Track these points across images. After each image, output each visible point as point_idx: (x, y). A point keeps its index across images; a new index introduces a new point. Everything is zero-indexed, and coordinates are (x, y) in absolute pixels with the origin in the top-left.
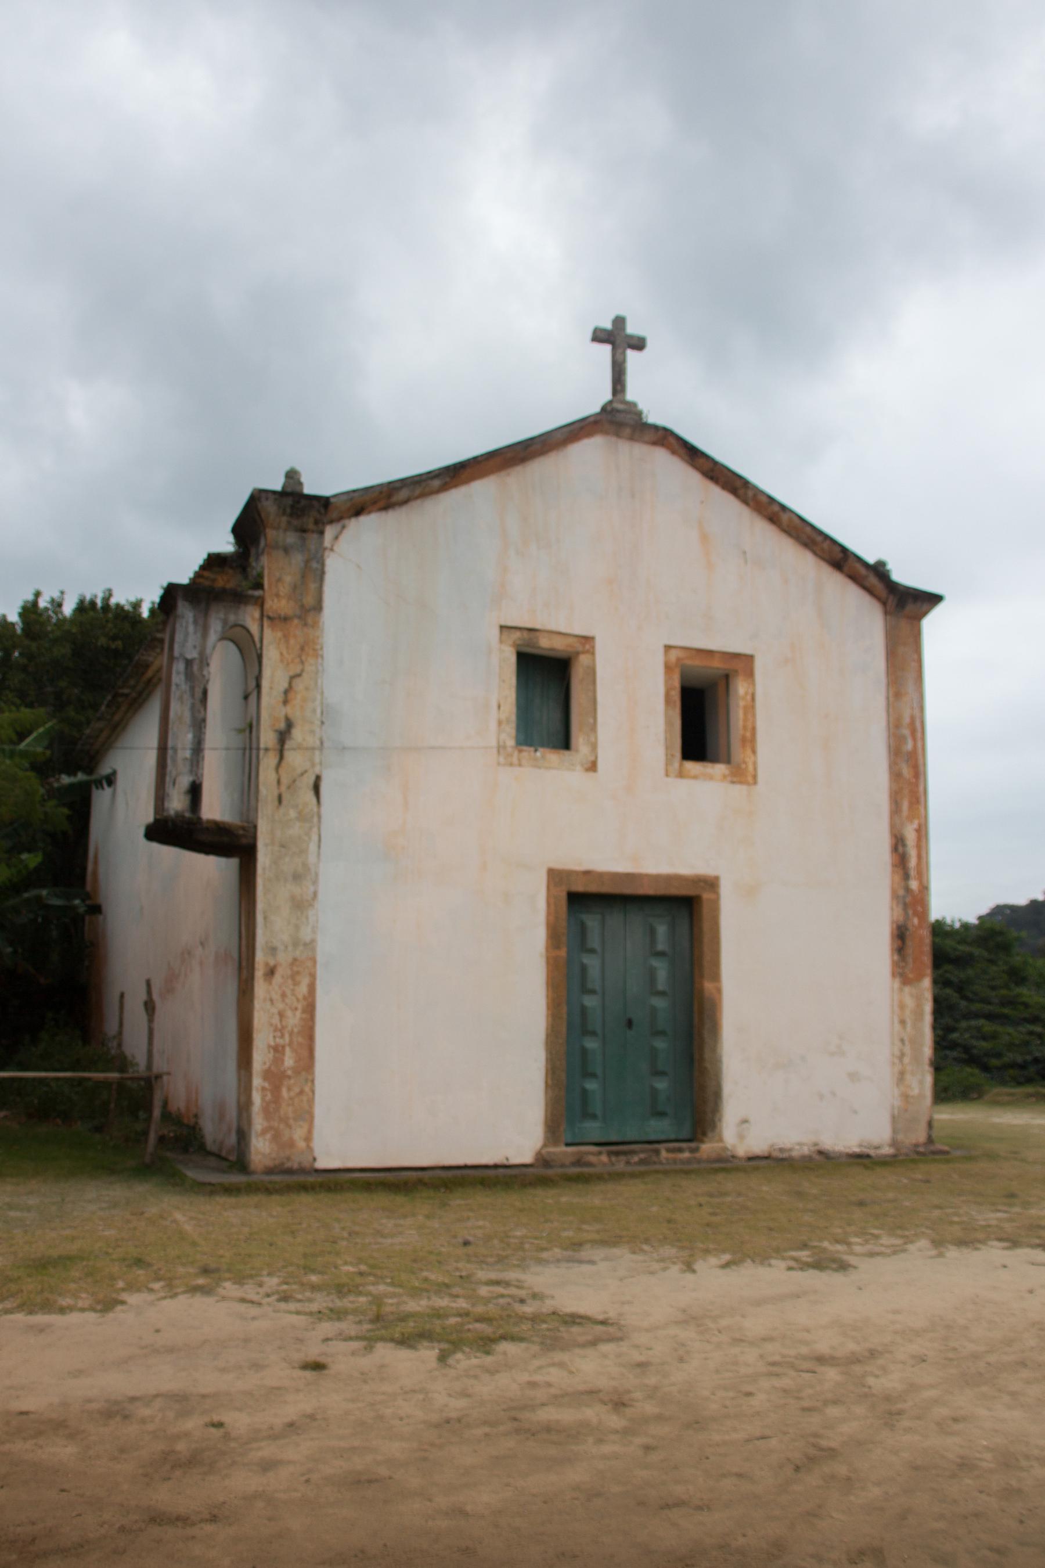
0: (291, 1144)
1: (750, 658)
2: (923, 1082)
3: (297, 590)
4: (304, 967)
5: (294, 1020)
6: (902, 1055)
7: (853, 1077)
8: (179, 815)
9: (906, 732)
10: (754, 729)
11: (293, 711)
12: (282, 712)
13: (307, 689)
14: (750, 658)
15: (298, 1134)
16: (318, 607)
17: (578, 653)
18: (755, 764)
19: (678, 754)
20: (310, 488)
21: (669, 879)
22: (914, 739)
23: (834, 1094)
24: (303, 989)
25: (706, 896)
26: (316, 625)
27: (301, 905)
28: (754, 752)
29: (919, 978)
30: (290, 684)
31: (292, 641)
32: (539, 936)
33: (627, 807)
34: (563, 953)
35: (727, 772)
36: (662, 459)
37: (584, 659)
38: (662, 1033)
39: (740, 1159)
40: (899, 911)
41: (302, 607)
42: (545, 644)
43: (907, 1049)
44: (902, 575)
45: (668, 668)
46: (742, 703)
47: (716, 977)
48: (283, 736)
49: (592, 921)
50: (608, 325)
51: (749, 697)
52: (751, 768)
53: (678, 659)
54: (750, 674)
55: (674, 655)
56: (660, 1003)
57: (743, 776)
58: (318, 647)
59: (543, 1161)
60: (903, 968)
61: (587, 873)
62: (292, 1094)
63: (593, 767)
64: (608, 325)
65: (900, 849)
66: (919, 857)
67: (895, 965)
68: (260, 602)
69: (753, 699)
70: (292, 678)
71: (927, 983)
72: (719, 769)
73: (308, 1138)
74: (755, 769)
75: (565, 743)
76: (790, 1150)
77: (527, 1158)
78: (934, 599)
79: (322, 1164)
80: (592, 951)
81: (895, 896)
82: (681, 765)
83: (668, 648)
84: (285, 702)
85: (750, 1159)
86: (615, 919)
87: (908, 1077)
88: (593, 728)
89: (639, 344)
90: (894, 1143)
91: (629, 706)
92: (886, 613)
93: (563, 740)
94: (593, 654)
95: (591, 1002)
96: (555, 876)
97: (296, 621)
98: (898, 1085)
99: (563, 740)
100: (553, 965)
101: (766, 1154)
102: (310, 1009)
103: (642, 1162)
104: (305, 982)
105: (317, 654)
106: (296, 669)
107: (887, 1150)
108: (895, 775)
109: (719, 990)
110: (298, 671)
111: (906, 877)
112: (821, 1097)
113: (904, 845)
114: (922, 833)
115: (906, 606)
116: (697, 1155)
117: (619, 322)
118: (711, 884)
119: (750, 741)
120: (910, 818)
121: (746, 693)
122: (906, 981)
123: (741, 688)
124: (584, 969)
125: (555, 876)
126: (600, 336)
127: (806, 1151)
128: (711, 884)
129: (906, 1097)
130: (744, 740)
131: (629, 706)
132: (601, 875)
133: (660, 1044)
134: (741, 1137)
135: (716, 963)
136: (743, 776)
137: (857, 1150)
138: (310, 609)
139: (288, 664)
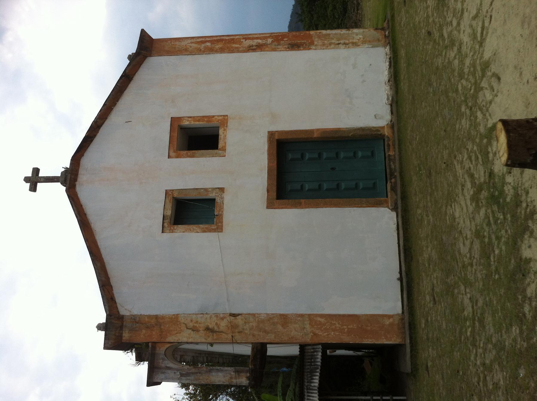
0: (391, 325)
2: (357, 33)
6: (345, 44)
7: (354, 66)
8: (248, 378)
9: (203, 45)
10: (203, 117)
12: (202, 333)
13: (192, 321)
15: (387, 322)
16: (156, 317)
17: (173, 197)
18: (218, 116)
19: (216, 151)
20: (103, 320)
21: (269, 154)
22: (206, 42)
23: (362, 75)
24: (322, 320)
25: (277, 137)
26: (163, 317)
28: (214, 116)
29: (310, 36)
30: (190, 329)
31: (171, 329)
33: (240, 172)
34: (303, 201)
35: (223, 129)
36: (85, 161)
37: (176, 195)
38: (337, 154)
39: (392, 118)
41: (156, 325)
42: (169, 213)
43: (342, 42)
44: (133, 49)
45: (178, 157)
46: (193, 123)
47: (312, 131)
50: (28, 185)
51: (190, 119)
52: (220, 118)
53: (174, 152)
54: (179, 119)
55: (172, 154)
57: (224, 120)
58: (173, 317)
59: (395, 209)
60: (306, 45)
61: (268, 191)
62: (369, 325)
63: (222, 190)
64: (28, 185)
65: (254, 47)
66: (257, 38)
67: (305, 49)
68: (154, 343)
69: (191, 117)
70: (187, 328)
71: (312, 32)
72: (221, 132)
73: (389, 317)
74: (221, 116)
75: (212, 201)
76: (388, 95)
77: (394, 214)
78: (143, 32)
79: (398, 309)
80: (302, 186)
81: (274, 50)
82: (221, 150)
83: (169, 157)
84: (198, 331)
85: (392, 113)
87: (355, 41)
88: (206, 190)
89: (36, 171)
90: (385, 46)
91: (195, 173)
92: (150, 56)
94: (173, 190)
96: (270, 205)
97: (162, 327)
98: (359, 46)
101: (390, 106)
103: (394, 163)
104: (319, 319)
105: (177, 316)
106: (183, 327)
107: (388, 49)
108: (222, 51)
109: (318, 130)
110: (184, 325)
112: (364, 81)
113: (252, 46)
114: (247, 37)
115: (147, 47)
116: (391, 138)
117: (27, 180)
118: (271, 134)
119: (209, 118)
120: (240, 43)
121: (188, 121)
122: (312, 43)
123: (186, 123)
124: (309, 190)
125: (270, 205)
126: (33, 188)
127: (388, 88)
128: (271, 134)
129: (364, 42)
130: (209, 121)
131: (195, 173)
132: (269, 185)
133: (342, 155)
134: (381, 118)
135: (306, 131)
136: (224, 120)
137: (388, 64)
139: (181, 330)
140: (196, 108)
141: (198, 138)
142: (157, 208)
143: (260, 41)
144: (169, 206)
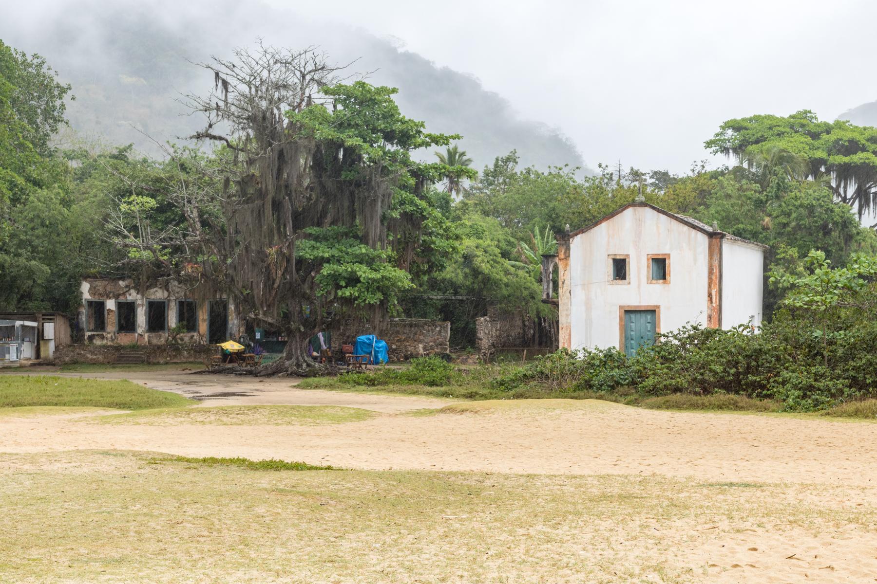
1: (669, 255)
3: (565, 253)
4: (569, 327)
5: (567, 337)
11: (565, 278)
14: (669, 255)
16: (569, 256)
21: (647, 306)
27: (567, 315)
32: (618, 320)
33: (639, 290)
40: (710, 312)
42: (618, 257)
48: (563, 283)
49: (633, 316)
54: (669, 258)
56: (649, 333)
63: (629, 283)
86: (638, 316)
91: (639, 268)
93: (624, 277)
95: (632, 333)
96: (621, 307)
99: (624, 277)
100: (621, 325)
102: (570, 335)
111: (712, 303)
118: (658, 307)
125: (621, 307)
128: (658, 307)
131: (639, 268)
138: (567, 256)
140: (673, 266)
141: (660, 267)
142: (620, 253)
143: (714, 299)
144: (622, 257)
